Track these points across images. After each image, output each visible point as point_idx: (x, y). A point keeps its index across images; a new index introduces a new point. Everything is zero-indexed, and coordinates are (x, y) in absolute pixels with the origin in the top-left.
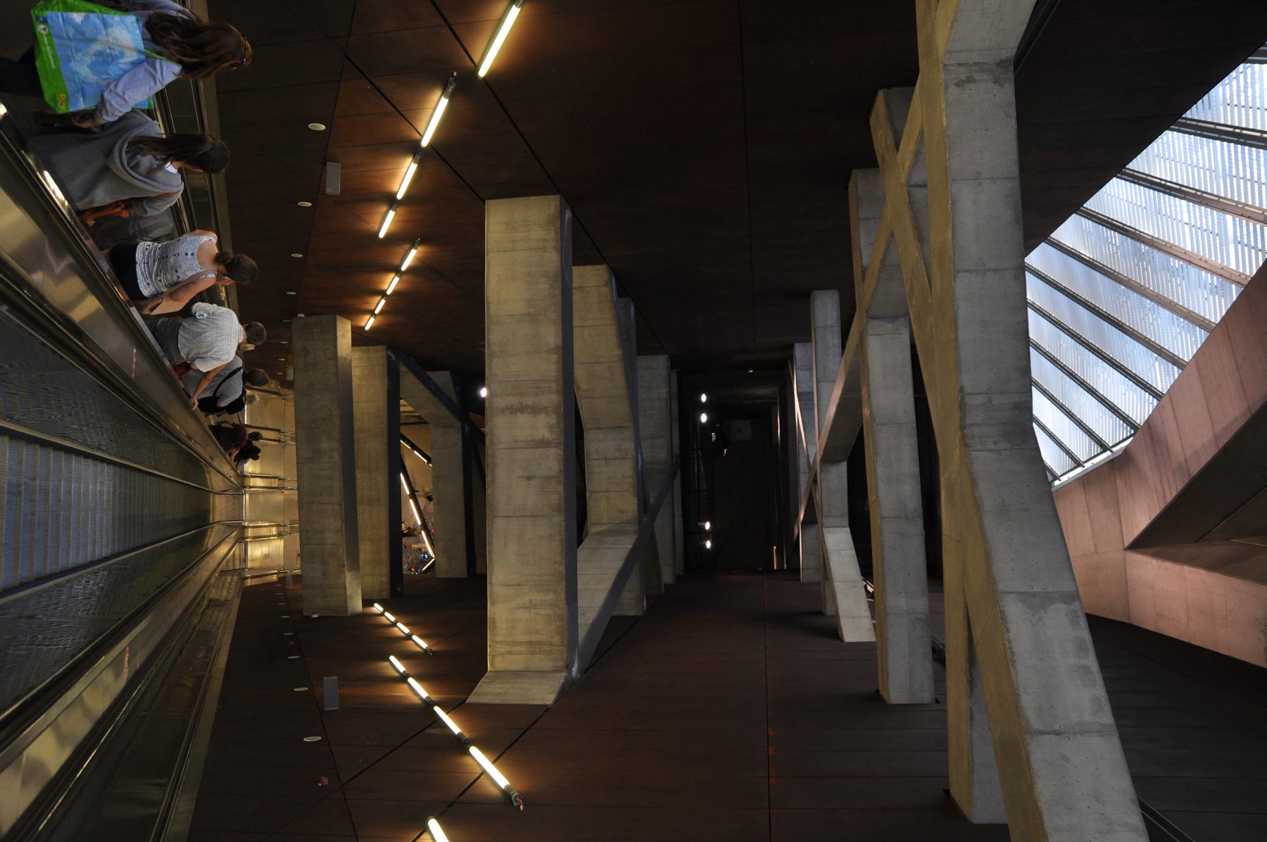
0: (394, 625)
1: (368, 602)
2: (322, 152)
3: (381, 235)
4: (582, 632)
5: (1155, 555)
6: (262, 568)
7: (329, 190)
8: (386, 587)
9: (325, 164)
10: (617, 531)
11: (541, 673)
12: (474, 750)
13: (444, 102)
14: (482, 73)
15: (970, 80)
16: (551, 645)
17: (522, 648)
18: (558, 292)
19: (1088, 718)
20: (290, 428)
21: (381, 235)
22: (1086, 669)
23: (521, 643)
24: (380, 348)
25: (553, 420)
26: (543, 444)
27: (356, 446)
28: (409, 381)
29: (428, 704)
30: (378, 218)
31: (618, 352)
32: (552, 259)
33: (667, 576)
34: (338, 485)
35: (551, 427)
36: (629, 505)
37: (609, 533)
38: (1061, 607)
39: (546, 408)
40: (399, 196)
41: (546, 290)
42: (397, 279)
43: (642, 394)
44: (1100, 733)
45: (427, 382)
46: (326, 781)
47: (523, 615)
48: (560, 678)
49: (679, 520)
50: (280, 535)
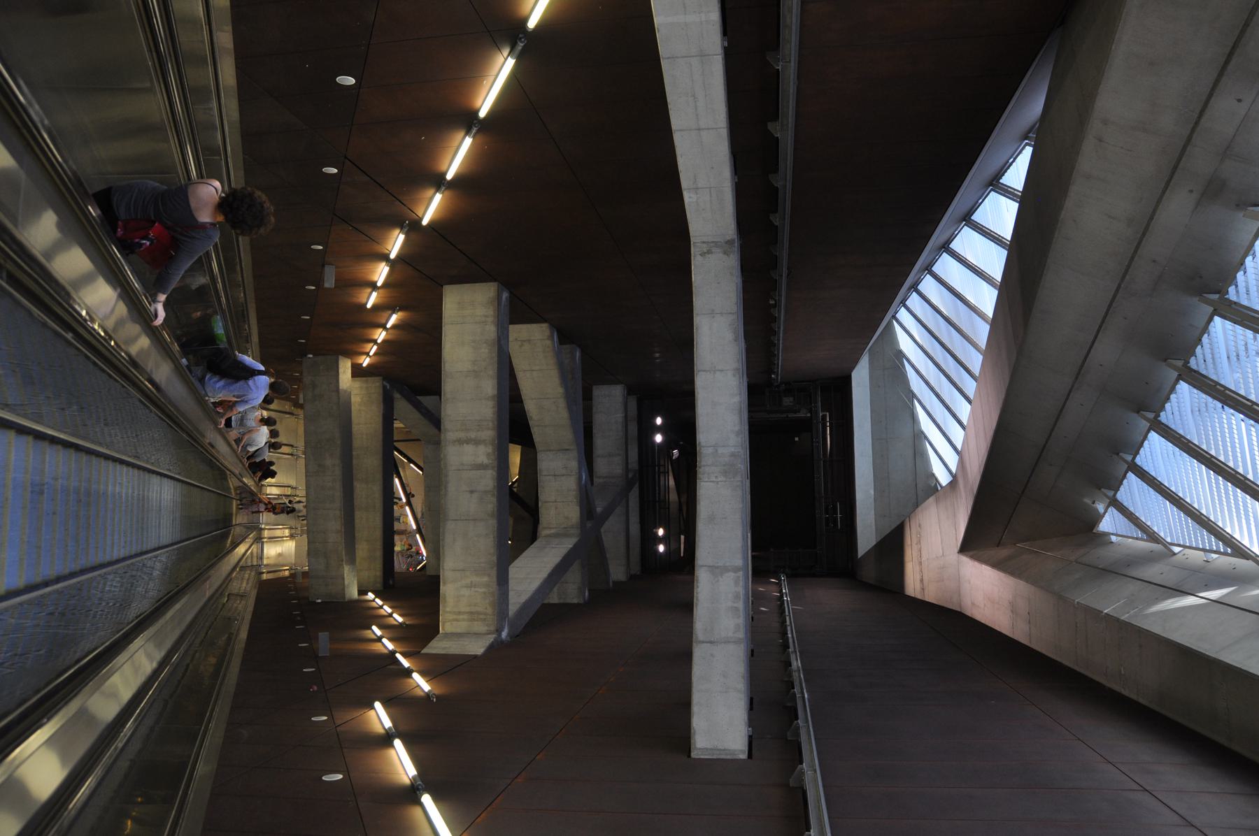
0: (381, 607)
1: (362, 592)
2: (321, 261)
3: (369, 306)
4: (513, 609)
5: (972, 557)
6: (275, 565)
7: (327, 285)
8: (380, 580)
9: (323, 266)
11: (477, 635)
12: (416, 676)
13: (402, 237)
14: (425, 222)
15: (709, 252)
16: (486, 614)
17: (465, 617)
18: (495, 355)
19: (730, 634)
20: (301, 444)
21: (369, 306)
22: (737, 609)
23: (464, 613)
24: (377, 379)
25: (490, 449)
27: (354, 462)
28: (401, 405)
29: (393, 653)
30: (366, 295)
31: (561, 390)
32: (491, 330)
33: (617, 572)
34: (338, 494)
35: (488, 455)
36: (573, 513)
37: (557, 535)
38: (732, 574)
40: (379, 284)
41: (486, 354)
42: (384, 333)
43: (599, 419)
45: (418, 406)
47: (466, 592)
48: (490, 639)
49: (635, 528)
50: (292, 536)
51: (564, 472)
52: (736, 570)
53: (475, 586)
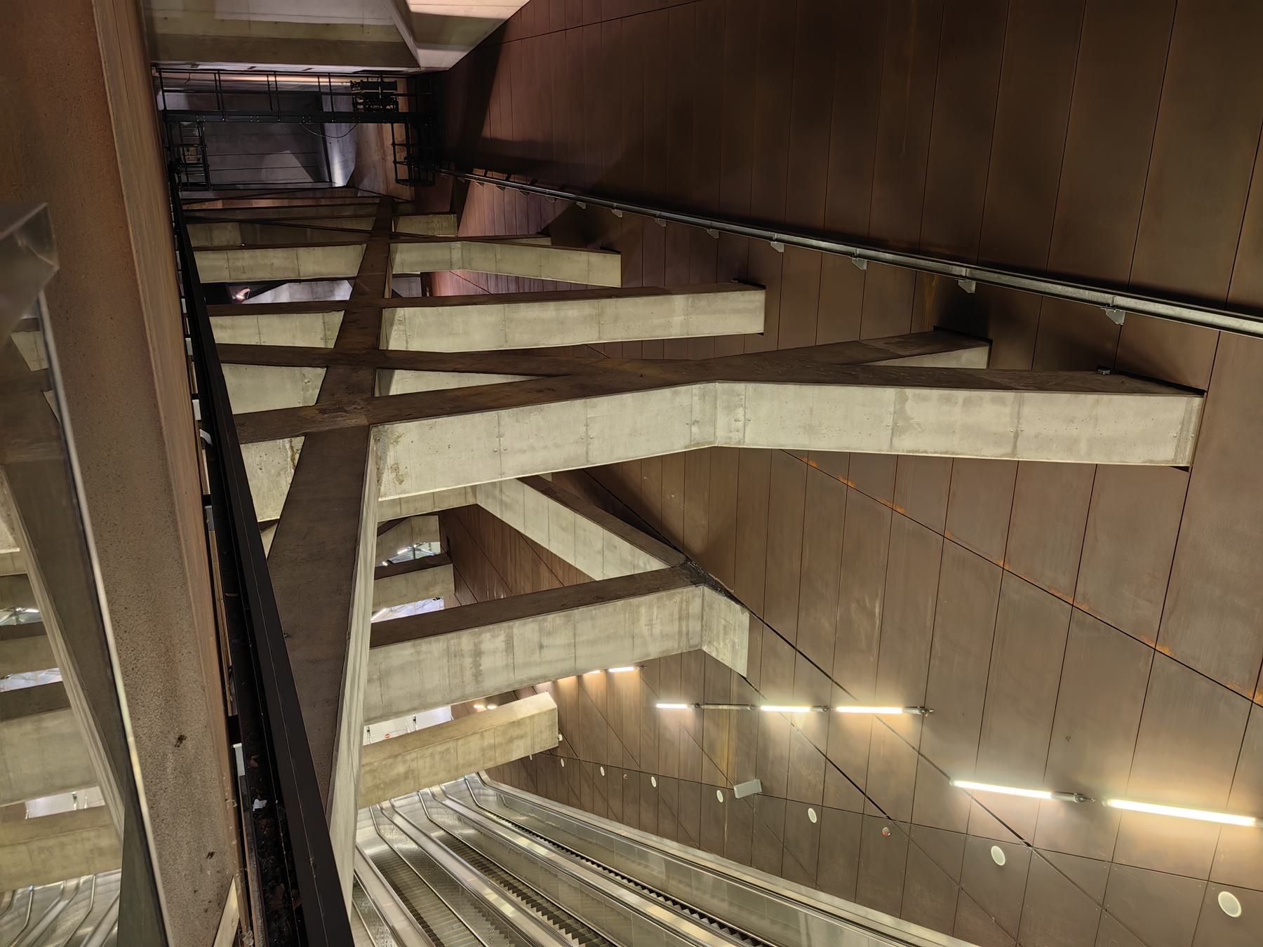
15: (396, 469)
17: (684, 624)
19: (1007, 410)
22: (967, 402)
23: (680, 626)
35: (493, 637)
38: (909, 406)
39: (475, 645)
46: (886, 829)
47: (657, 630)
52: (904, 400)
53: (651, 620)
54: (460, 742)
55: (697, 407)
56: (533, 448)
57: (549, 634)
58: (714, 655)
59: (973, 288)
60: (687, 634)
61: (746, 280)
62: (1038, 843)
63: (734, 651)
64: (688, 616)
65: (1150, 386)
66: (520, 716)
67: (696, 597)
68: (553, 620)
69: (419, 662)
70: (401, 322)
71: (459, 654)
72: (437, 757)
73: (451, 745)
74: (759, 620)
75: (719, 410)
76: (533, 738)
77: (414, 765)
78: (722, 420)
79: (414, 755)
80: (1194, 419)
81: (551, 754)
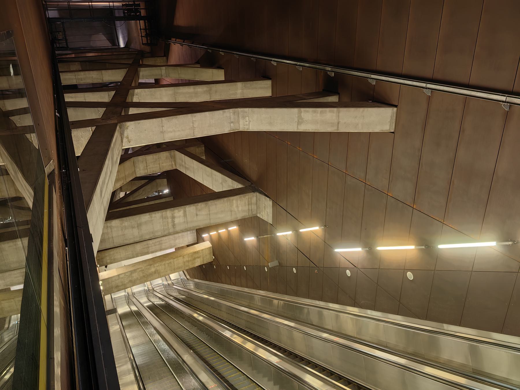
10: (174, 158)
15: (127, 138)
17: (250, 206)
22: (321, 112)
26: (185, 212)
35: (179, 211)
37: (175, 161)
38: (302, 114)
39: (172, 214)
44: (339, 113)
47: (240, 209)
51: (145, 162)
52: (300, 113)
54: (175, 260)
55: (232, 117)
56: (174, 131)
57: (200, 210)
58: (261, 217)
59: (333, 75)
60: (252, 210)
61: (265, 77)
62: (359, 267)
63: (268, 215)
64: (251, 203)
65: (383, 105)
66: (198, 250)
67: (254, 197)
68: (201, 205)
69: (152, 220)
70: (137, 95)
71: (166, 218)
72: (167, 265)
73: (172, 260)
74: (275, 203)
75: (240, 118)
76: (203, 258)
77: (158, 268)
78: (241, 122)
79: (157, 264)
80: (395, 115)
81: (210, 264)
